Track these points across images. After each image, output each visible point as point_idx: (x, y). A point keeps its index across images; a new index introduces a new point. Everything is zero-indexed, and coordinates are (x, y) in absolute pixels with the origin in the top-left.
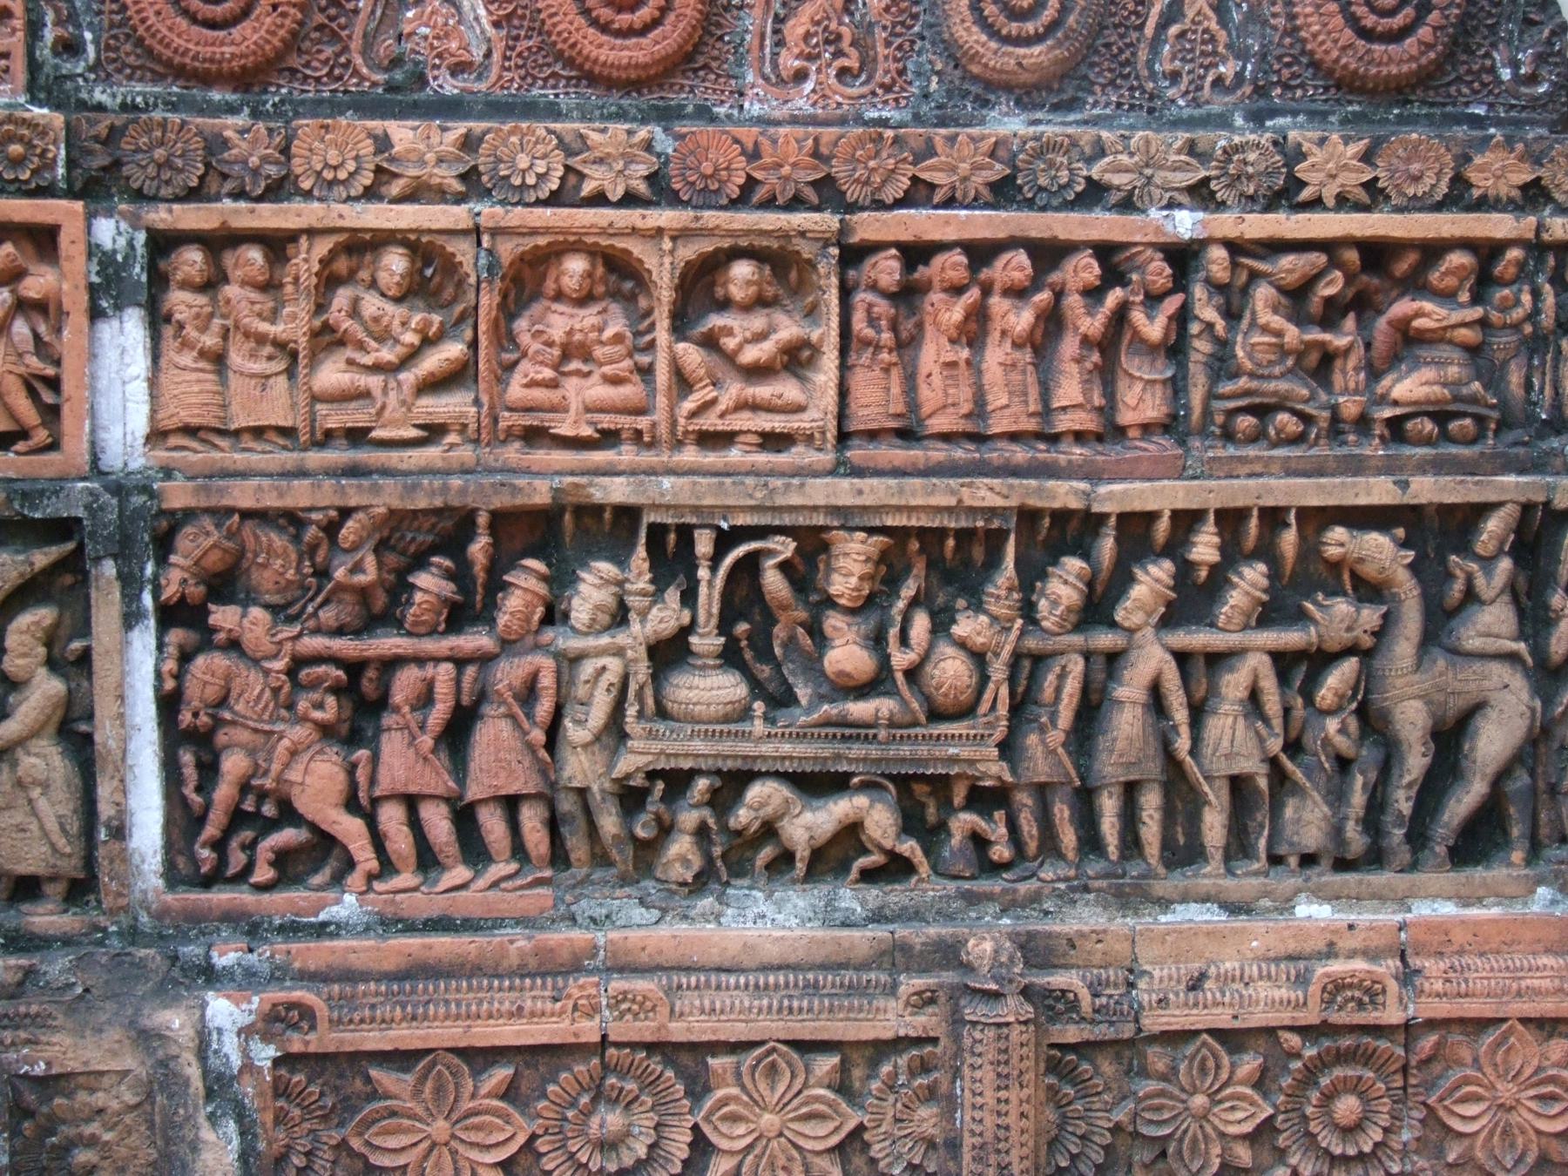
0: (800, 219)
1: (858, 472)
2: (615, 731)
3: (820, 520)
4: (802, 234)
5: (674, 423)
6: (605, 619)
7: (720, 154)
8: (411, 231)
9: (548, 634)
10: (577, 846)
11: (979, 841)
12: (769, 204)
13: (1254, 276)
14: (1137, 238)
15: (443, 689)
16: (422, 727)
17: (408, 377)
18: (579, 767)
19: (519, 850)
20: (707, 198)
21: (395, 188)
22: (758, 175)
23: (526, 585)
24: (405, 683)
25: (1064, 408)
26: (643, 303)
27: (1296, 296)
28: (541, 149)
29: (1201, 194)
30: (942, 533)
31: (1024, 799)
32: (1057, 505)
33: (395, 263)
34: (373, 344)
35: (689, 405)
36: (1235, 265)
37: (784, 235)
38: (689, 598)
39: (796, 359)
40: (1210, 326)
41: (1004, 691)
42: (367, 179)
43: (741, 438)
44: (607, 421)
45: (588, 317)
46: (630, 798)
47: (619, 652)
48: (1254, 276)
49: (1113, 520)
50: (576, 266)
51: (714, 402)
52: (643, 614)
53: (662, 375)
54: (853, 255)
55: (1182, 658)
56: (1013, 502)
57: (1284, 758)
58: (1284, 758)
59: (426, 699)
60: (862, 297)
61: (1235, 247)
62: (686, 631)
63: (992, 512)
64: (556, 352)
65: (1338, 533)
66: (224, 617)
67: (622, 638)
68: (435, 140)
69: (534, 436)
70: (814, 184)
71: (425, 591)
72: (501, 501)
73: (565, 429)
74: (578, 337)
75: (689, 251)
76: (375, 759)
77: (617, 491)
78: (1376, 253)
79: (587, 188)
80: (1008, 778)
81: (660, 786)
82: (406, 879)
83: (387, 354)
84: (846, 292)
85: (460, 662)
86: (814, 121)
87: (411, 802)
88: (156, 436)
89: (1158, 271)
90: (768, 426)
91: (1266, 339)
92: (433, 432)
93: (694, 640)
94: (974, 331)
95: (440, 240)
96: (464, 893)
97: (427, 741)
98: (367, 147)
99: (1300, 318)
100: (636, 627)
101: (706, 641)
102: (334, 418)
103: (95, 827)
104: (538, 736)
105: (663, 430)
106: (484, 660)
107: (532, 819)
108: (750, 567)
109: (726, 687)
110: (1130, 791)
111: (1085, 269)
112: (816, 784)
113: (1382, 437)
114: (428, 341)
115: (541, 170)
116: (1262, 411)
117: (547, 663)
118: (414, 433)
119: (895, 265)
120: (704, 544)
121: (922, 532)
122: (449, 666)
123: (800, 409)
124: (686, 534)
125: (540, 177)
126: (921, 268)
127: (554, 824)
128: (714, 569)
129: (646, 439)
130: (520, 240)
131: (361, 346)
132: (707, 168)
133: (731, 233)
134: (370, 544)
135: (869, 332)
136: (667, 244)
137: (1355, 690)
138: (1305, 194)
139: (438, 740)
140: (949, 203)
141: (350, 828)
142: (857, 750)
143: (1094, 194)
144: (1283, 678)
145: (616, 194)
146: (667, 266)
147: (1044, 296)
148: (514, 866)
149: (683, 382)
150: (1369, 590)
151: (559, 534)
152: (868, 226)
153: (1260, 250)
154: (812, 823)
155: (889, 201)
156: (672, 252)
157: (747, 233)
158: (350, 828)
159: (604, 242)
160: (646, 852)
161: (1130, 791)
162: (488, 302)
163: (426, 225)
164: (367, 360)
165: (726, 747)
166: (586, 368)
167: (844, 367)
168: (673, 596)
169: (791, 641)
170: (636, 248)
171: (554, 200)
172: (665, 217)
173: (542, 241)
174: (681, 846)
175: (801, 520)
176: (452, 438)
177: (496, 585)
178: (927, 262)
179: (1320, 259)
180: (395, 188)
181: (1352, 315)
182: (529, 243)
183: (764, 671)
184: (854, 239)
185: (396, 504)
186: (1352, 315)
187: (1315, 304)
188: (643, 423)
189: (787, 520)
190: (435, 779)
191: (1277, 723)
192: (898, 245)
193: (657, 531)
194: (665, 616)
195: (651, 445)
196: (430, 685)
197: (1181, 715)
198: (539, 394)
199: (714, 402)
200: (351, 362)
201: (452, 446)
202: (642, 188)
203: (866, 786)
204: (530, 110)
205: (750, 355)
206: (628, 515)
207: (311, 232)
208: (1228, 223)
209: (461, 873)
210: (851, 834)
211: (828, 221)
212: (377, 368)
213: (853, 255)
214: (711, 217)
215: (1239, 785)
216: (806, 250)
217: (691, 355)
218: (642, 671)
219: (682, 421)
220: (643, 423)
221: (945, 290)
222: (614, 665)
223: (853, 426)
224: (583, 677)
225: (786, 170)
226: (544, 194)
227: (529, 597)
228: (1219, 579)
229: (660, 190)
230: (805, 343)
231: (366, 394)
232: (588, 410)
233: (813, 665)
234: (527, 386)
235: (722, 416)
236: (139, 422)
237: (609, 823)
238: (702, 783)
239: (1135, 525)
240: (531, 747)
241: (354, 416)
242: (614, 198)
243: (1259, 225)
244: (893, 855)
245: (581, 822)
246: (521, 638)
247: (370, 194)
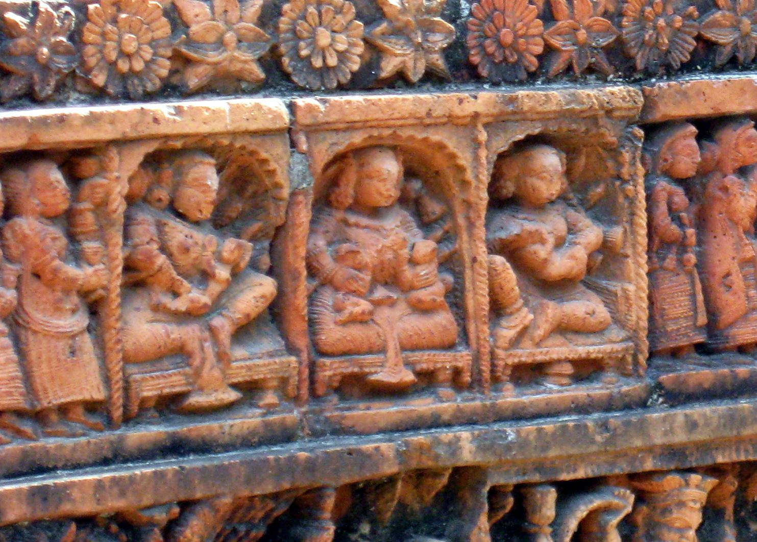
0: (592, 94)
4: (609, 113)
21: (193, 80)
22: (556, 42)
28: (341, 20)
33: (205, 180)
42: (164, 68)
43: (557, 369)
44: (425, 360)
53: (477, 299)
73: (384, 376)
74: (389, 255)
79: (388, 67)
95: (252, 144)
102: (152, 385)
118: (232, 395)
129: (467, 378)
136: (483, 136)
140: (734, 64)
145: (416, 73)
155: (676, 65)
164: (181, 305)
176: (270, 398)
180: (193, 80)
198: (356, 333)
201: (270, 409)
202: (439, 61)
207: (122, 143)
211: (618, 92)
219: (500, 353)
226: (346, 78)
229: (460, 68)
232: (403, 348)
241: (170, 381)
247: (170, 89)
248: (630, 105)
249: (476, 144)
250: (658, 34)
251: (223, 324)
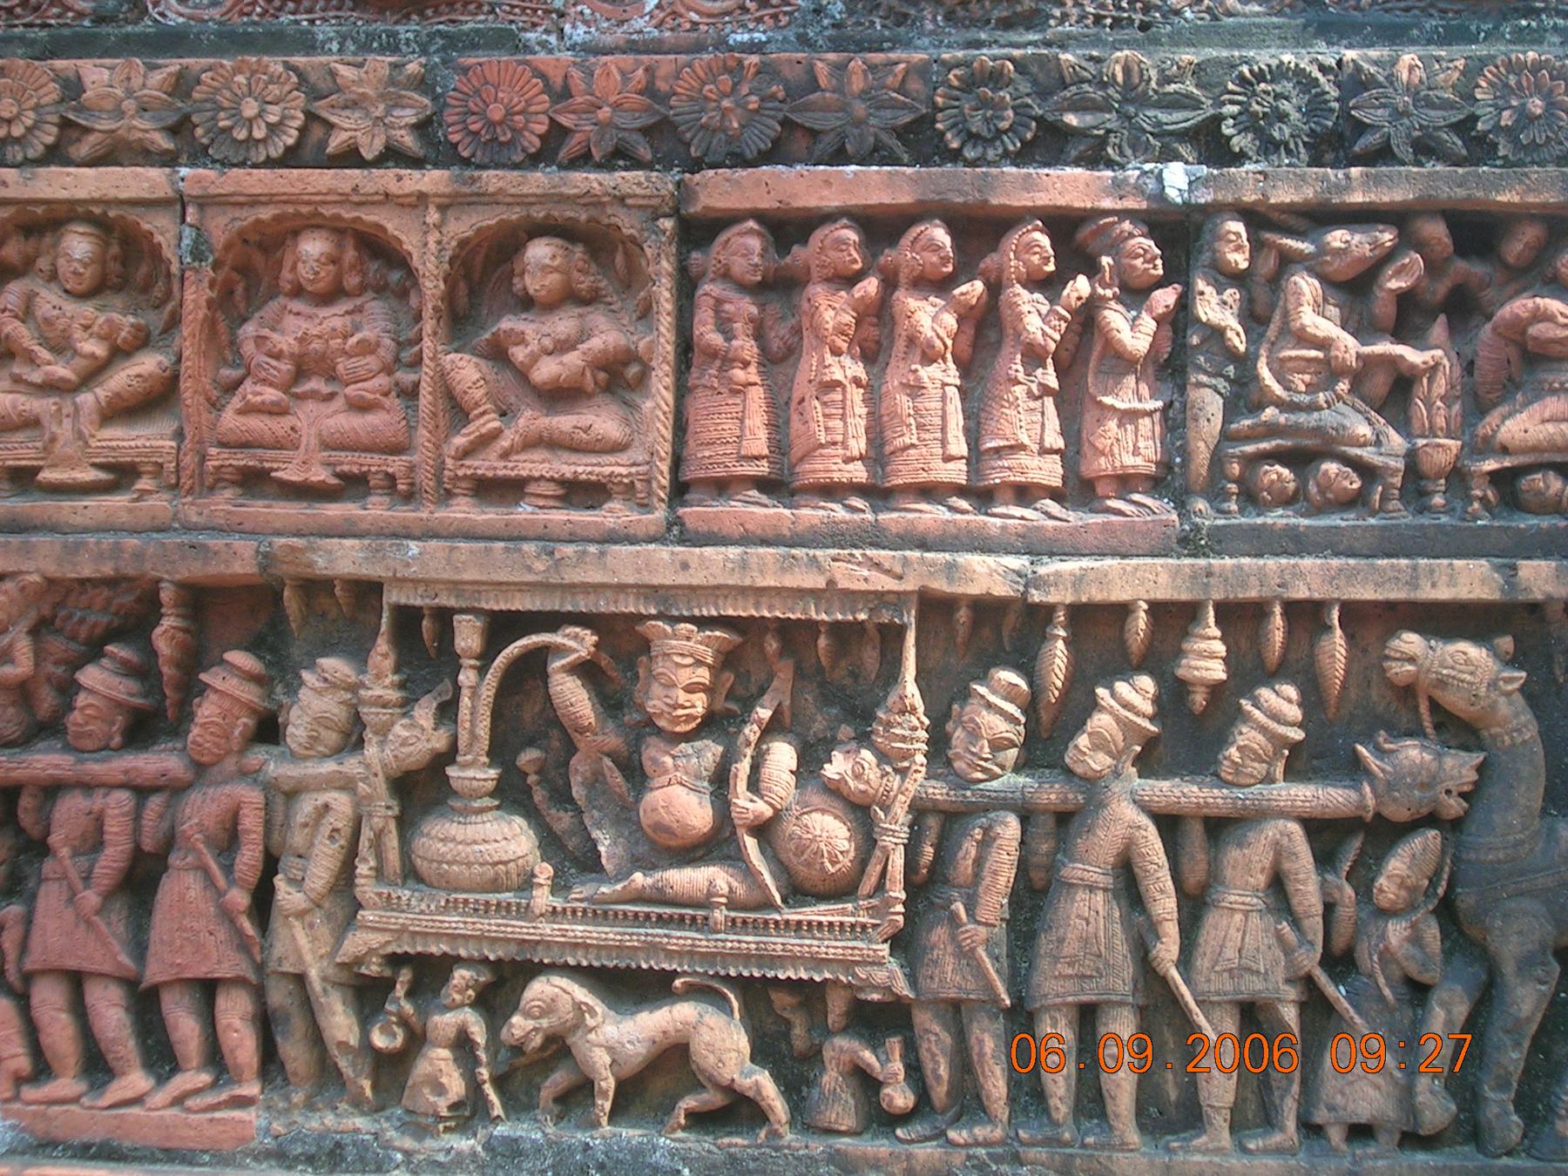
0: (627, 180)
1: (689, 538)
3: (629, 606)
4: (621, 200)
5: (441, 467)
6: (332, 738)
7: (508, 91)
8: (94, 201)
9: (259, 755)
10: (294, 1051)
11: (867, 1083)
12: (583, 160)
13: (1287, 261)
14: (1107, 204)
15: (116, 827)
16: (87, 878)
17: (86, 399)
18: (304, 945)
19: (215, 1057)
20: (498, 152)
21: (83, 150)
22: (565, 120)
23: (231, 681)
25: (997, 450)
26: (414, 301)
27: (1352, 289)
28: (275, 90)
29: (1211, 146)
30: (812, 626)
31: (924, 1019)
32: (974, 589)
34: (44, 354)
35: (460, 441)
36: (1257, 246)
37: (590, 200)
38: (447, 711)
39: (617, 377)
40: (1217, 332)
41: (898, 860)
43: (532, 488)
44: (350, 462)
45: (333, 318)
47: (347, 785)
48: (1287, 261)
49: (1061, 616)
50: (313, 247)
51: (495, 435)
52: (384, 731)
54: (699, 231)
55: (1169, 823)
56: (910, 585)
57: (1322, 978)
58: (1322, 978)
59: (94, 841)
60: (710, 289)
61: (1258, 219)
62: (449, 755)
63: (879, 599)
64: (286, 366)
65: (1410, 642)
67: (352, 765)
68: (136, 82)
69: (254, 481)
70: (645, 131)
71: (91, 691)
72: (194, 570)
73: (291, 474)
74: (316, 345)
75: (462, 226)
76: (28, 921)
77: (345, 558)
78: (1476, 231)
79: (335, 142)
80: (903, 988)
81: (405, 975)
82: (67, 1084)
83: (62, 371)
84: (687, 286)
85: (142, 792)
86: (655, 47)
87: (76, 981)
90: (568, 471)
91: (1313, 353)
92: (122, 475)
93: (452, 771)
95: (132, 215)
96: (135, 1110)
97: (91, 898)
98: (52, 92)
100: (371, 751)
101: (475, 773)
104: (240, 898)
105: (424, 478)
106: (176, 790)
107: (234, 1012)
108: (533, 667)
109: (509, 839)
110: (1087, 1015)
112: (630, 986)
113: (1483, 500)
114: (119, 353)
115: (272, 119)
117: (252, 796)
119: (755, 243)
120: (468, 636)
121: (785, 629)
122: (123, 796)
123: (617, 448)
124: (444, 617)
125: (273, 128)
126: (795, 248)
127: (266, 1024)
128: (482, 671)
130: (238, 213)
131: (31, 359)
132: (496, 112)
133: (521, 200)
134: (24, 625)
135: (716, 339)
136: (433, 216)
137: (1433, 883)
138: (1369, 140)
139: (108, 896)
142: (682, 938)
144: (1325, 860)
146: (432, 246)
147: (974, 289)
148: (205, 1078)
149: (457, 410)
150: (1456, 729)
151: (272, 617)
152: (719, 190)
153: (1302, 224)
154: (618, 1036)
156: (438, 227)
157: (543, 198)
159: (348, 214)
160: (392, 1069)
161: (1087, 1015)
162: (195, 297)
163: (113, 193)
164: (36, 377)
165: (491, 925)
166: (325, 389)
167: (682, 391)
168: (424, 713)
169: (596, 780)
170: (393, 224)
171: (291, 158)
172: (432, 180)
173: (266, 214)
174: (439, 1061)
175: (604, 606)
176: (144, 483)
177: (191, 689)
178: (804, 240)
179: (1387, 237)
180: (83, 150)
181: (1442, 318)
182: (249, 216)
183: (562, 821)
184: (695, 209)
185: (52, 570)
186: (1442, 318)
187: (1383, 307)
188: (396, 464)
189: (583, 605)
190: (104, 948)
191: (1315, 924)
192: (758, 215)
193: (407, 618)
194: (414, 736)
195: (409, 497)
196: (99, 820)
197: (1165, 905)
198: (259, 425)
199: (495, 435)
200: (17, 380)
201: (144, 493)
202: (409, 141)
203: (701, 992)
204: (276, 42)
205: (547, 370)
206: (367, 591)
208: (1249, 180)
209: (136, 1080)
210: (674, 1057)
211: (662, 183)
212: (51, 387)
213: (699, 231)
214: (492, 179)
215: (1252, 1015)
216: (628, 223)
217: (467, 371)
218: (383, 810)
219: (449, 462)
220: (396, 464)
221: (828, 280)
222: (341, 802)
223: (690, 473)
224: (300, 819)
225: (605, 113)
226: (276, 151)
227: (227, 704)
228: (1223, 703)
230: (628, 357)
231: (32, 423)
232: (326, 446)
233: (626, 816)
234: (240, 412)
235: (505, 455)
237: (341, 1023)
238: (461, 975)
239: (1096, 622)
240: (227, 915)
242: (368, 155)
243: (1292, 186)
244: (729, 1089)
245: (298, 1024)
246: (220, 759)
247: (55, 155)
248: (648, 192)
249: (426, 229)
250: (723, 116)
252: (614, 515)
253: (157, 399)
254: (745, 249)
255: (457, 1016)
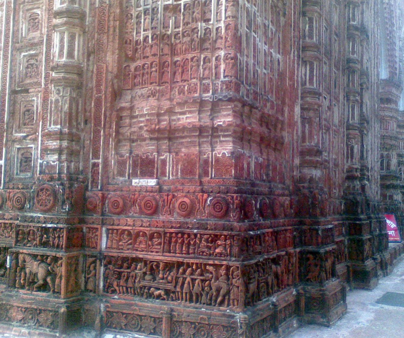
2: (139, 282)
17: (126, 244)
24: (123, 274)
33: (126, 232)
46: (141, 288)
66: (109, 266)
78: (216, 236)
88: (106, 248)
89: (193, 237)
94: (176, 242)
99: (208, 242)
102: (120, 247)
103: (96, 286)
111: (186, 236)
116: (203, 252)
141: (117, 288)
143: (188, 228)
158: (117, 288)
194: (144, 270)
236: (105, 246)
243: (202, 232)
251: (126, 244)
252: (159, 254)
253: (130, 244)
254: (168, 235)
255: (146, 291)
